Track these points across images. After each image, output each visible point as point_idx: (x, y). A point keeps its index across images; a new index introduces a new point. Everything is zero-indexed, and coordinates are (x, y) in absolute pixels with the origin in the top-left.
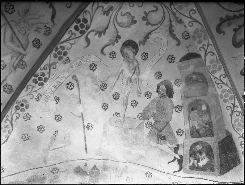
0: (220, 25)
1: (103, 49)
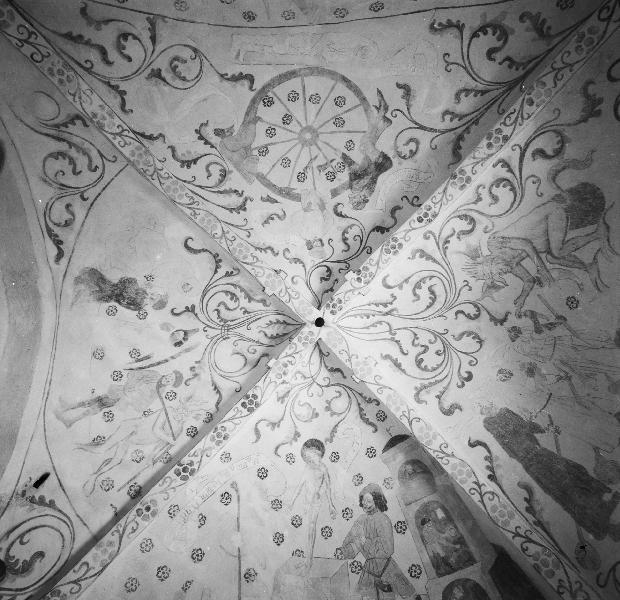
0: (418, 394)
1: (277, 448)
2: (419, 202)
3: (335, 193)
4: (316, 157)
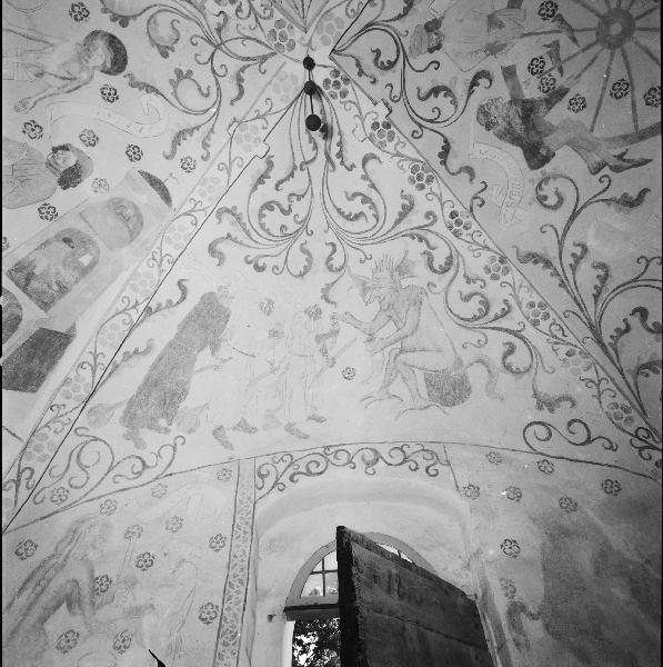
0: (228, 211)
2: (476, 209)
3: (509, 73)
4: (574, 40)
